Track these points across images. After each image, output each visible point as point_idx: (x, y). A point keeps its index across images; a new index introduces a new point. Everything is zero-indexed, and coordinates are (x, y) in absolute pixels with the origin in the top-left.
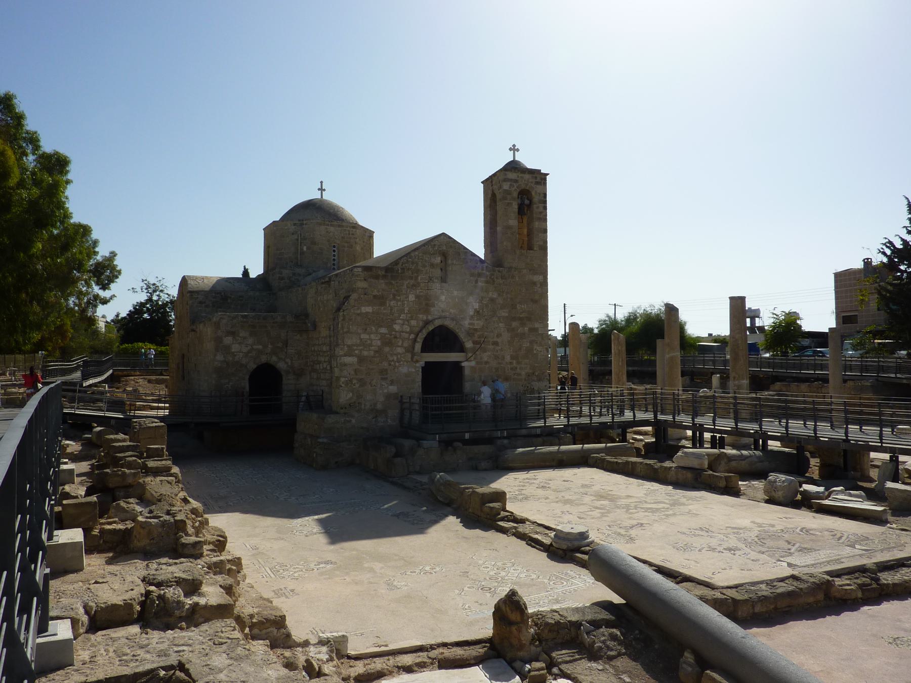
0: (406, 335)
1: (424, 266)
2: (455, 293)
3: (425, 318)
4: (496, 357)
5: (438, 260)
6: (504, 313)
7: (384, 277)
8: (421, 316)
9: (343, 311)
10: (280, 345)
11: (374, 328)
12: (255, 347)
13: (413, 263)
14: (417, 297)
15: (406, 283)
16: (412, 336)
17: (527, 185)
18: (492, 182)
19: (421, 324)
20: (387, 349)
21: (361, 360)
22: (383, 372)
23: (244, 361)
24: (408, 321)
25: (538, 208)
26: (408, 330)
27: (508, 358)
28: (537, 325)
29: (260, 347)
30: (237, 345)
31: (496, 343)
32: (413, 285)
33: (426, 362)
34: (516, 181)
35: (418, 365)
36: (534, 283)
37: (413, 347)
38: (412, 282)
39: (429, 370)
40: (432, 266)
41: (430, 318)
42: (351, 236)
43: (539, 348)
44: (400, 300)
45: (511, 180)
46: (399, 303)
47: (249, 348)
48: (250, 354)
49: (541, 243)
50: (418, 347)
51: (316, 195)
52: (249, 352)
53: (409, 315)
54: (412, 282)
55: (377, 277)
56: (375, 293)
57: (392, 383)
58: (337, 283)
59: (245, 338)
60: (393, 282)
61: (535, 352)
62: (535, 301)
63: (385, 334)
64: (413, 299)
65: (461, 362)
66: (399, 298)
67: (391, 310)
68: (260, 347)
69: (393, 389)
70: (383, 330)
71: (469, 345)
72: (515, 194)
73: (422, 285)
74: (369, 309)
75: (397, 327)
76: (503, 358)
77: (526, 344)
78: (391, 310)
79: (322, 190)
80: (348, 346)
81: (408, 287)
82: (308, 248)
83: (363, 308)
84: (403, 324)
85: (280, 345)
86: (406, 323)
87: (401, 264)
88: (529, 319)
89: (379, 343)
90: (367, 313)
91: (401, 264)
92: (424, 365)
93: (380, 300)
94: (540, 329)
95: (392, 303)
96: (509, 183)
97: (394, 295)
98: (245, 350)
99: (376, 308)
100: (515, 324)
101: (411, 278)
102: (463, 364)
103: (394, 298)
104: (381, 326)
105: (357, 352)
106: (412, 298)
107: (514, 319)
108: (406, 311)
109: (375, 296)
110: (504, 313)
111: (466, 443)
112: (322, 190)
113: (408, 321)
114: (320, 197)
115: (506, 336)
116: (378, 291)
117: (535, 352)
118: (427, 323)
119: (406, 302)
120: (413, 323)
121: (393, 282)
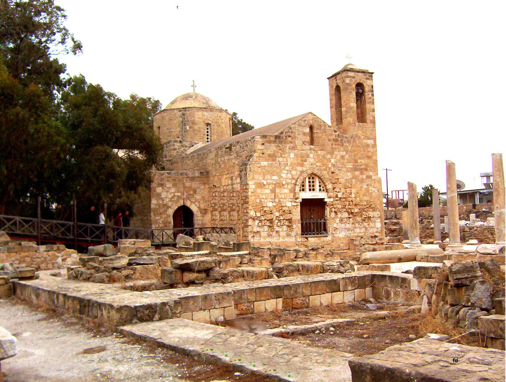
0: (289, 181)
1: (299, 134)
2: (319, 152)
5: (308, 130)
7: (275, 142)
9: (250, 165)
10: (192, 192)
11: (269, 176)
12: (176, 194)
13: (292, 132)
14: (295, 155)
15: (288, 145)
16: (294, 181)
17: (361, 80)
18: (336, 78)
19: (298, 173)
25: (368, 95)
26: (291, 177)
28: (371, 173)
29: (179, 194)
30: (165, 193)
33: (303, 199)
34: (354, 77)
35: (297, 201)
36: (368, 146)
38: (292, 145)
40: (304, 134)
41: (304, 169)
42: (219, 118)
43: (373, 189)
44: (284, 157)
45: (350, 77)
46: (285, 159)
47: (172, 195)
48: (173, 199)
49: (372, 118)
51: (190, 91)
52: (173, 197)
53: (291, 167)
54: (292, 145)
55: (270, 142)
56: (269, 152)
59: (170, 188)
60: (280, 145)
61: (370, 192)
62: (369, 157)
63: (276, 180)
64: (293, 156)
65: (324, 199)
66: (284, 156)
67: (280, 163)
68: (179, 194)
72: (354, 86)
73: (298, 147)
75: (284, 175)
77: (365, 186)
79: (194, 86)
82: (190, 128)
83: (262, 163)
84: (287, 174)
85: (192, 192)
86: (289, 173)
87: (284, 133)
88: (366, 170)
90: (265, 166)
91: (284, 133)
92: (301, 201)
93: (272, 157)
94: (373, 176)
95: (280, 159)
96: (349, 79)
98: (170, 196)
100: (357, 173)
101: (291, 142)
102: (326, 200)
103: (281, 157)
104: (274, 175)
106: (292, 155)
107: (356, 169)
108: (289, 165)
110: (350, 166)
112: (194, 86)
113: (290, 172)
114: (193, 92)
116: (271, 151)
117: (370, 192)
118: (302, 172)
119: (288, 159)
120: (294, 172)
121: (280, 145)
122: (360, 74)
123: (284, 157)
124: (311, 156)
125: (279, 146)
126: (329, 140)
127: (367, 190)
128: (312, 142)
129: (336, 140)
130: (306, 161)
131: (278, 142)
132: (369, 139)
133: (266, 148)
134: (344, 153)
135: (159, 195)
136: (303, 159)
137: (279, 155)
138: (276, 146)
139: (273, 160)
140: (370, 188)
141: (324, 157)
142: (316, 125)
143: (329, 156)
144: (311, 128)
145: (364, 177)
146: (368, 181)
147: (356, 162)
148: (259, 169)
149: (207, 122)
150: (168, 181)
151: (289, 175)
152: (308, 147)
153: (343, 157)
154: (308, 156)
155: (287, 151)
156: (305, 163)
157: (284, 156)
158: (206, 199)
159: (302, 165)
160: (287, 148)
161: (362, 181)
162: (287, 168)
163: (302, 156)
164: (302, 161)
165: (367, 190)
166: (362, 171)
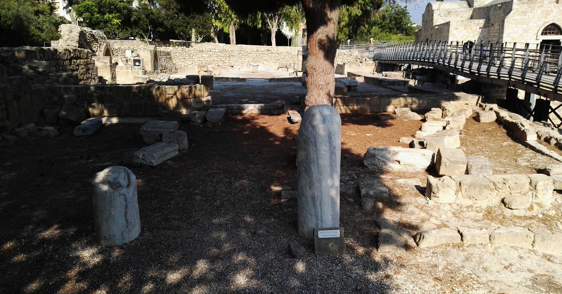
3: (544, 21)
7: (527, 3)
12: (465, 34)
14: (542, 11)
15: (537, 5)
16: (538, 29)
19: (542, 23)
20: (525, 34)
24: (536, 22)
29: (468, 34)
32: (541, 6)
41: (547, 20)
44: (533, 13)
46: (533, 14)
47: (463, 35)
50: (540, 32)
52: (463, 36)
56: (522, 10)
58: (505, 6)
67: (529, 17)
68: (468, 34)
70: (524, 26)
74: (519, 17)
78: (529, 17)
80: (508, 33)
81: (538, 7)
86: (535, 23)
89: (522, 32)
93: (524, 13)
95: (530, 14)
97: (531, 11)
99: (522, 17)
105: (511, 35)
106: (539, 11)
109: (522, 12)
113: (536, 22)
116: (524, 9)
118: (545, 23)
120: (539, 23)
123: (533, 13)
124: (555, 11)
125: (531, 6)
130: (549, 15)
131: (530, 3)
133: (520, 7)
135: (454, 35)
136: (547, 14)
137: (530, 11)
138: (528, 6)
139: (524, 15)
148: (513, 21)
150: (461, 26)
151: (535, 24)
152: (553, 5)
154: (552, 11)
155: (536, 9)
156: (549, 16)
157: (533, 12)
158: (486, 37)
159: (546, 18)
160: (536, 7)
162: (534, 20)
163: (547, 12)
164: (546, 15)
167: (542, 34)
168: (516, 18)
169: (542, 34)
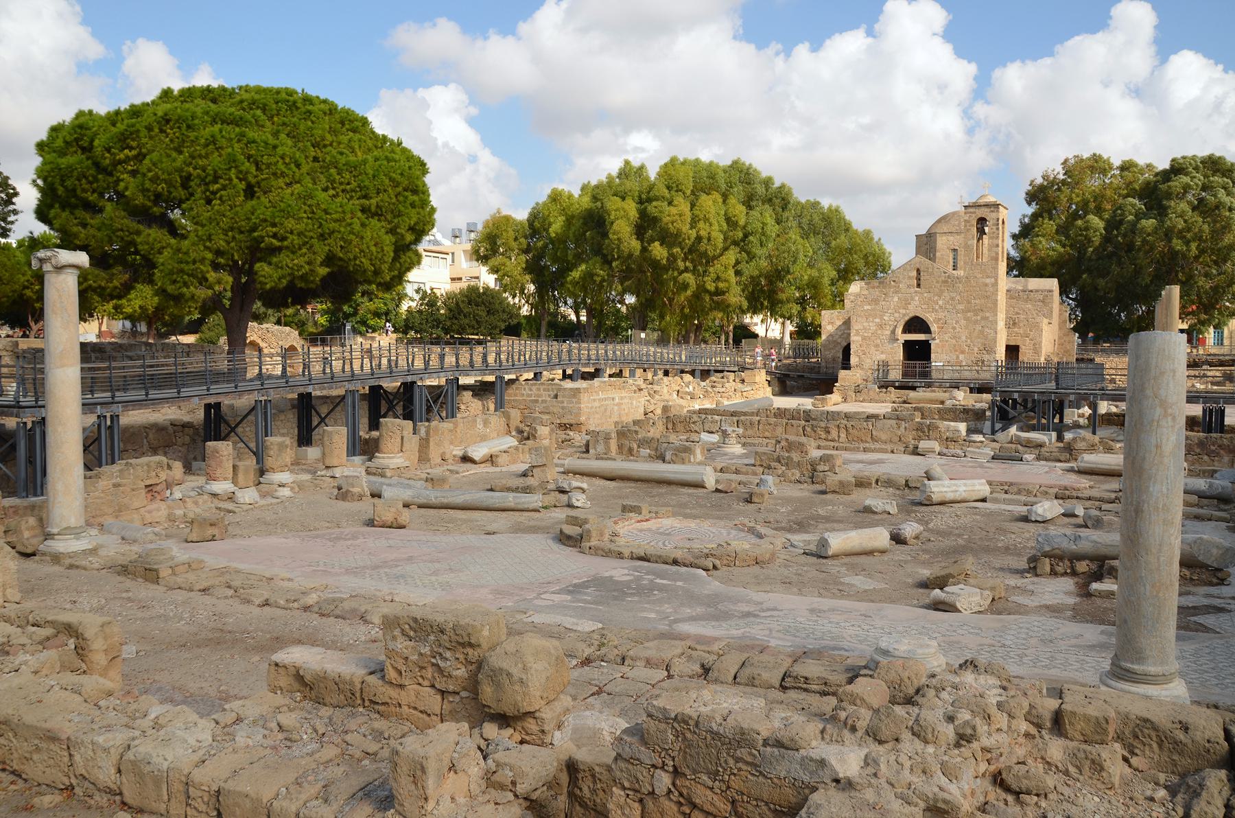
1: (904, 278)
4: (955, 337)
5: (914, 273)
6: (961, 307)
8: (901, 311)
20: (879, 332)
21: (864, 338)
22: (877, 346)
23: (839, 341)
27: (964, 338)
28: (988, 314)
31: (954, 328)
36: (986, 285)
37: (893, 332)
39: (908, 345)
40: (910, 278)
50: (899, 330)
55: (873, 288)
57: (882, 353)
69: (883, 357)
70: (877, 320)
71: (932, 329)
74: (869, 307)
76: (960, 338)
77: (978, 328)
93: (876, 301)
100: (969, 314)
106: (896, 299)
111: (896, 388)
115: (963, 322)
118: (904, 315)
122: (983, 209)
126: (937, 282)
127: (982, 332)
128: (919, 285)
129: (946, 282)
132: (988, 277)
134: (954, 295)
136: (906, 303)
140: (986, 330)
141: (930, 299)
142: (922, 269)
143: (936, 298)
144: (918, 271)
145: (979, 318)
146: (983, 323)
147: (969, 302)
149: (952, 247)
153: (953, 299)
161: (976, 322)
165: (982, 332)
166: (976, 312)
167: (904, 332)
168: (866, 308)
169: (904, 332)
